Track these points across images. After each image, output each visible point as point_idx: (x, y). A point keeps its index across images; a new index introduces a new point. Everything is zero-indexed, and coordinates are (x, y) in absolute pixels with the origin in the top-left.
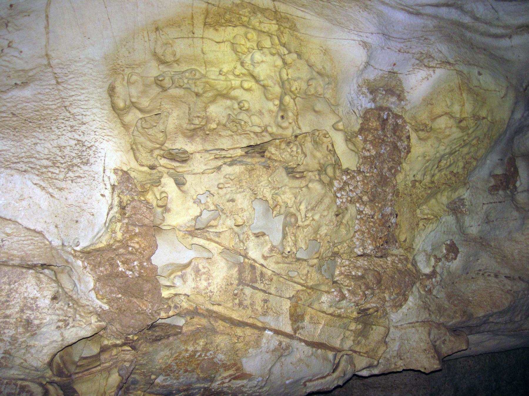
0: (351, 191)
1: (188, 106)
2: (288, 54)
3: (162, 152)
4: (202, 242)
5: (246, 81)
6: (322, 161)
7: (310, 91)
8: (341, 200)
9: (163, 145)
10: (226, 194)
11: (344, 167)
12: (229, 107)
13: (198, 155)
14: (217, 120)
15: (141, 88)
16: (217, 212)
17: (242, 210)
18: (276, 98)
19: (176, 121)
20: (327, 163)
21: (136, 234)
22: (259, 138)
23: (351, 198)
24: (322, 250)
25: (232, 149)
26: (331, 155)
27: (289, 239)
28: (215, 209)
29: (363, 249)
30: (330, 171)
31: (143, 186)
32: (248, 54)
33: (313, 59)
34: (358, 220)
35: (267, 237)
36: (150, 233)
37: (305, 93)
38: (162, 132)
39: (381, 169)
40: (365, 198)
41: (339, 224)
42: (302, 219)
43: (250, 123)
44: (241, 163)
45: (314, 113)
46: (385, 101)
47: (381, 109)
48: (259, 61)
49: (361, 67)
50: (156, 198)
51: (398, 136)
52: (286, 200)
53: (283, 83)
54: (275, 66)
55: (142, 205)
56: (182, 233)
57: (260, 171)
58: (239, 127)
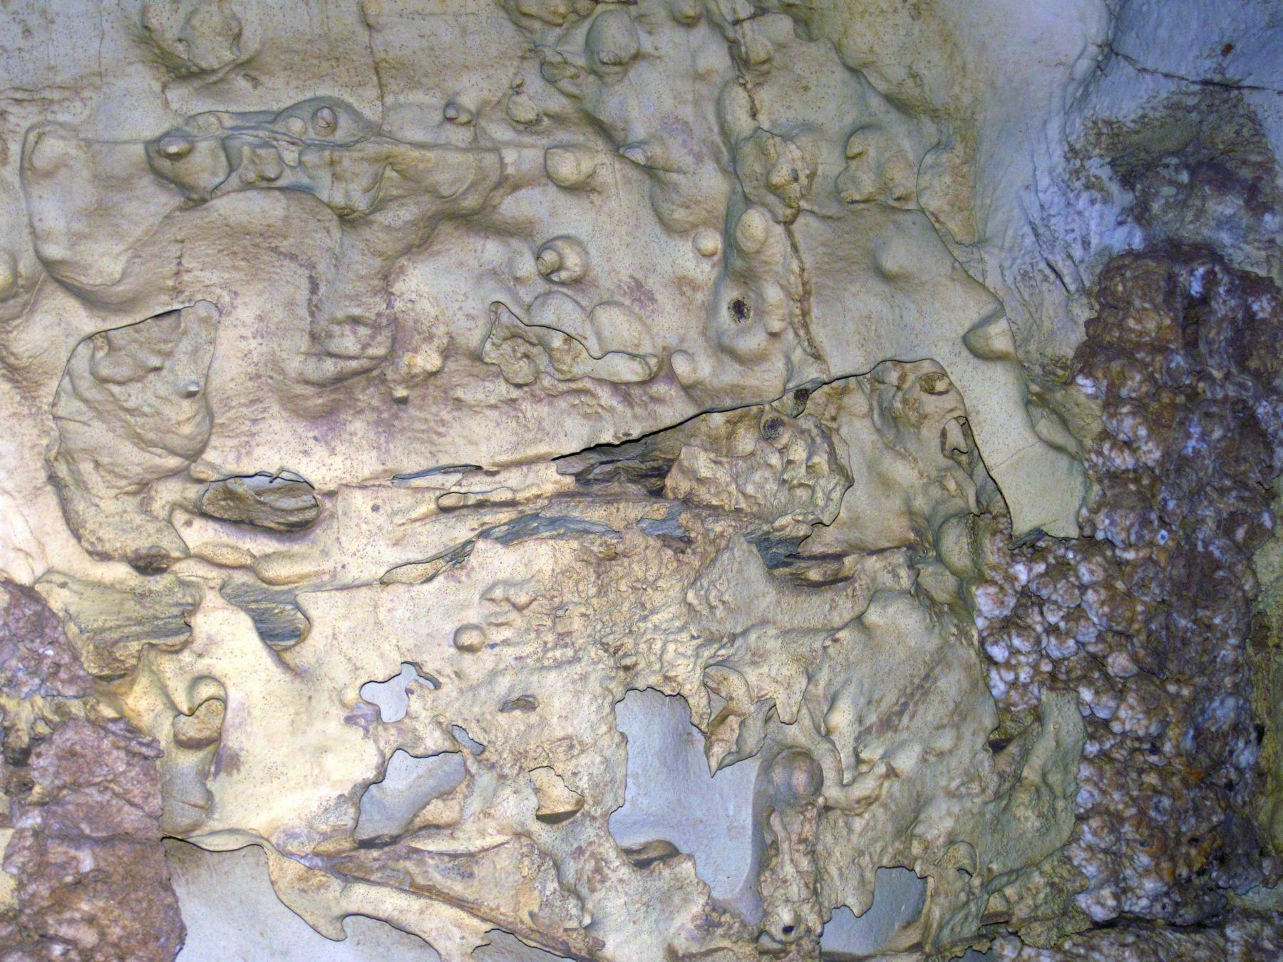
0: (1052, 630)
1: (307, 273)
2: (752, 17)
3: (193, 492)
4: (390, 902)
5: (567, 147)
6: (920, 503)
7: (856, 182)
8: (1010, 676)
9: (195, 455)
10: (494, 674)
11: (1024, 523)
12: (494, 273)
13: (360, 502)
14: (440, 330)
15: (85, 193)
16: (457, 757)
17: (571, 744)
18: (705, 223)
19: (253, 344)
20: (943, 510)
21: (80, 883)
22: (638, 410)
23: (1056, 663)
24: (937, 913)
25: (518, 464)
26: (960, 474)
27: (789, 870)
28: (447, 745)
29: (1116, 896)
30: (955, 545)
31: (105, 651)
32: (574, 25)
33: (861, 40)
34: (1091, 761)
35: (687, 866)
36: (149, 873)
37: (836, 193)
38: (191, 395)
39: (1191, 526)
40: (1119, 663)
41: (1007, 786)
42: (840, 771)
43: (592, 343)
44: (560, 527)
45: (877, 286)
46: (1190, 216)
47: (1177, 252)
48: (625, 56)
49: (1084, 65)
50: (173, 706)
51: (1257, 375)
52: (769, 689)
53: (734, 149)
54: (699, 77)
55: (106, 744)
56: (293, 868)
57: (647, 560)
58: (543, 362)
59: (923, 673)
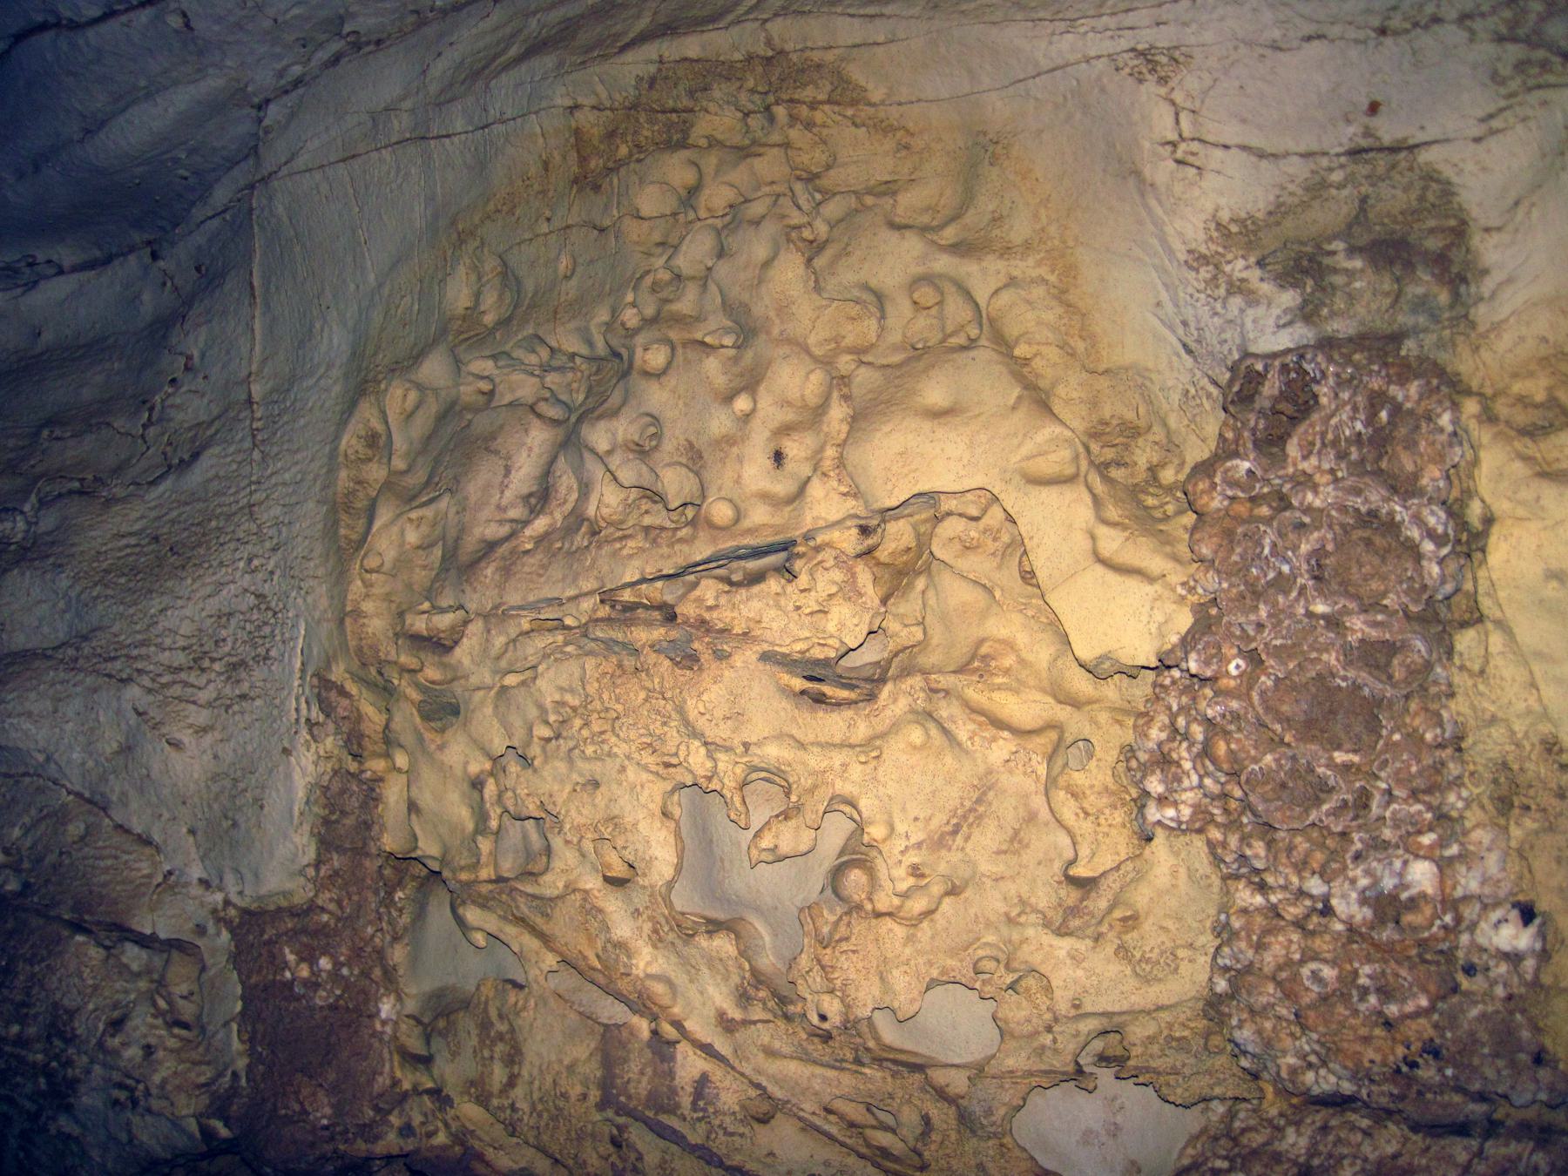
59: (975, 796)
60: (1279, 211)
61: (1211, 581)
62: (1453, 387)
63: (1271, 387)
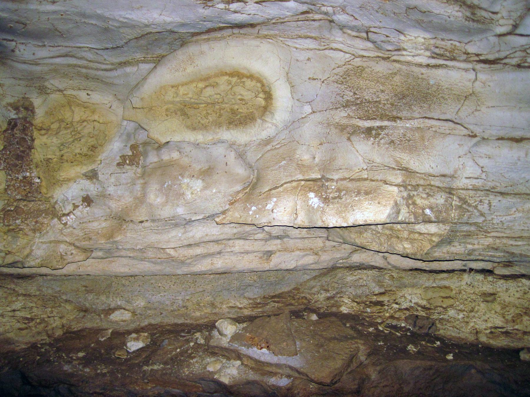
60: (14, 103)
61: (6, 143)
62: (32, 125)
63: (13, 123)
